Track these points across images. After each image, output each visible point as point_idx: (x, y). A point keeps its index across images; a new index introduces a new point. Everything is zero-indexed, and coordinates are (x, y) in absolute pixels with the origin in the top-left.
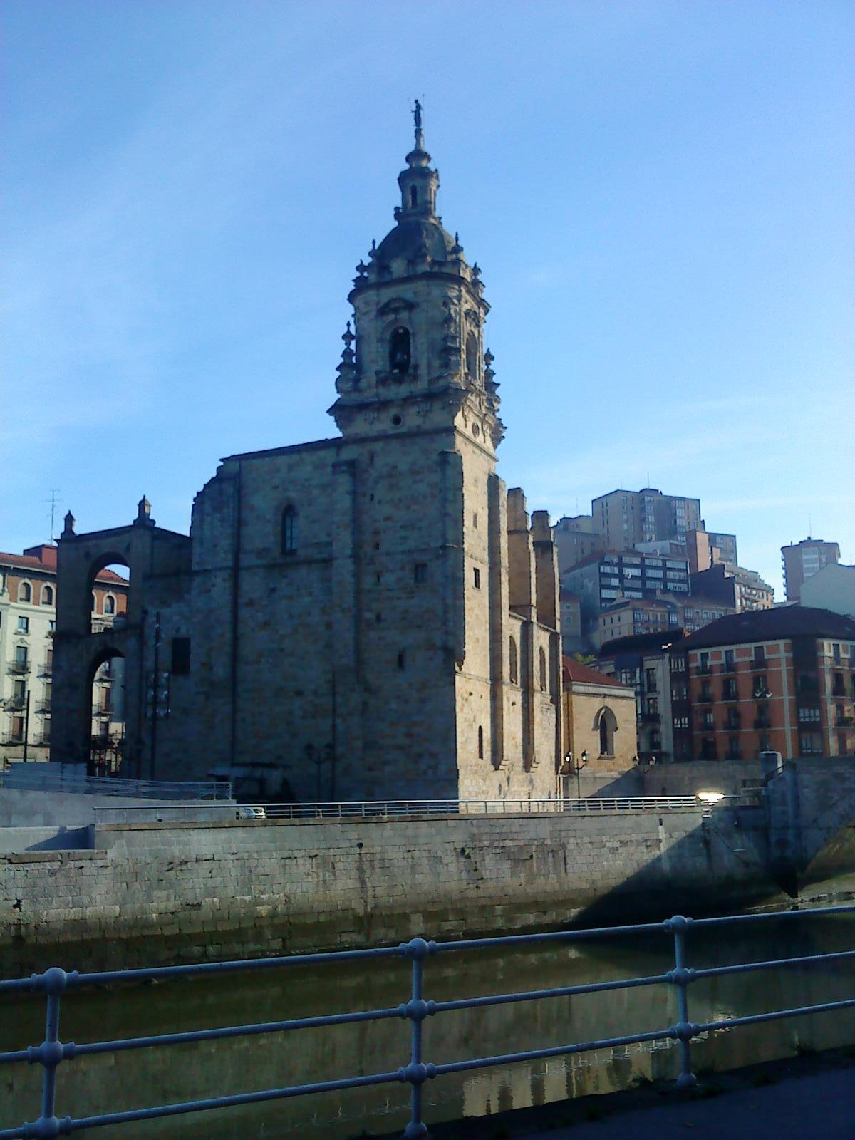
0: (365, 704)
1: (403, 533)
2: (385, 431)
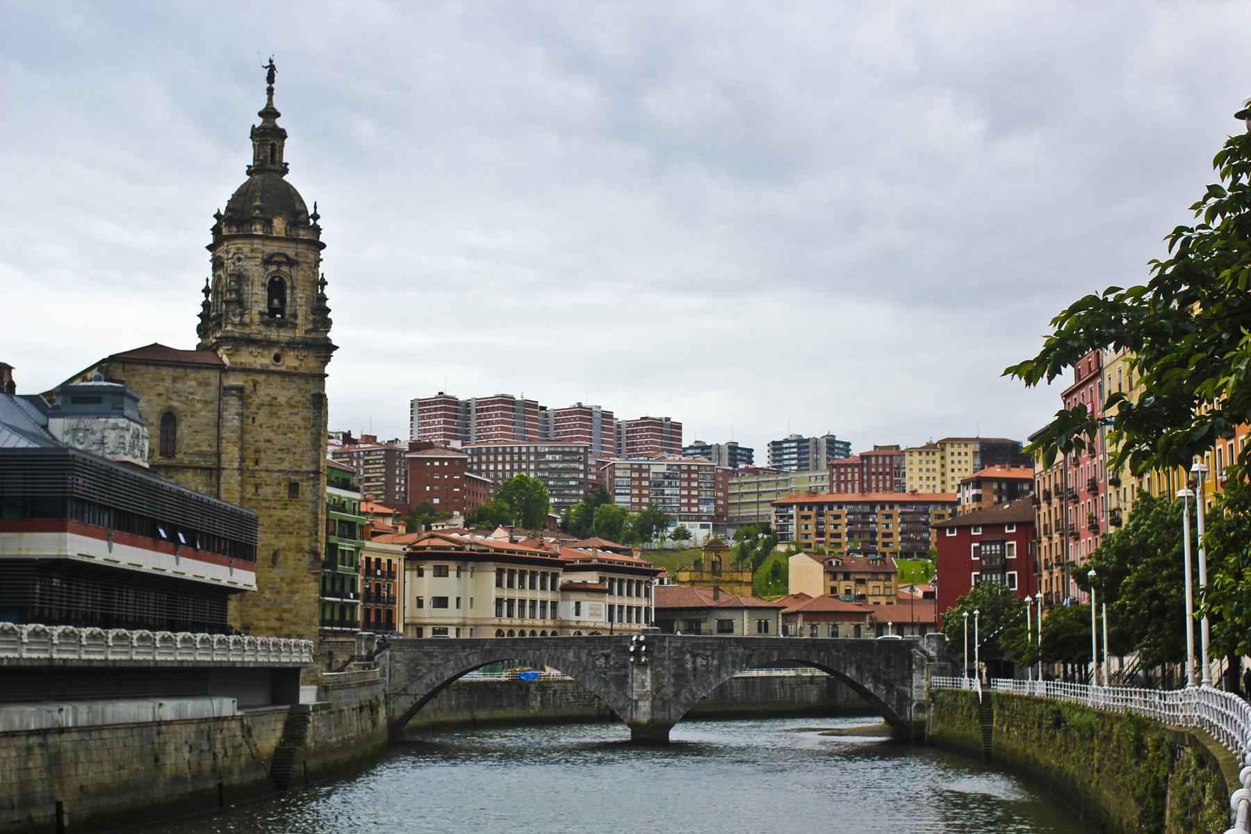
2: (266, 365)
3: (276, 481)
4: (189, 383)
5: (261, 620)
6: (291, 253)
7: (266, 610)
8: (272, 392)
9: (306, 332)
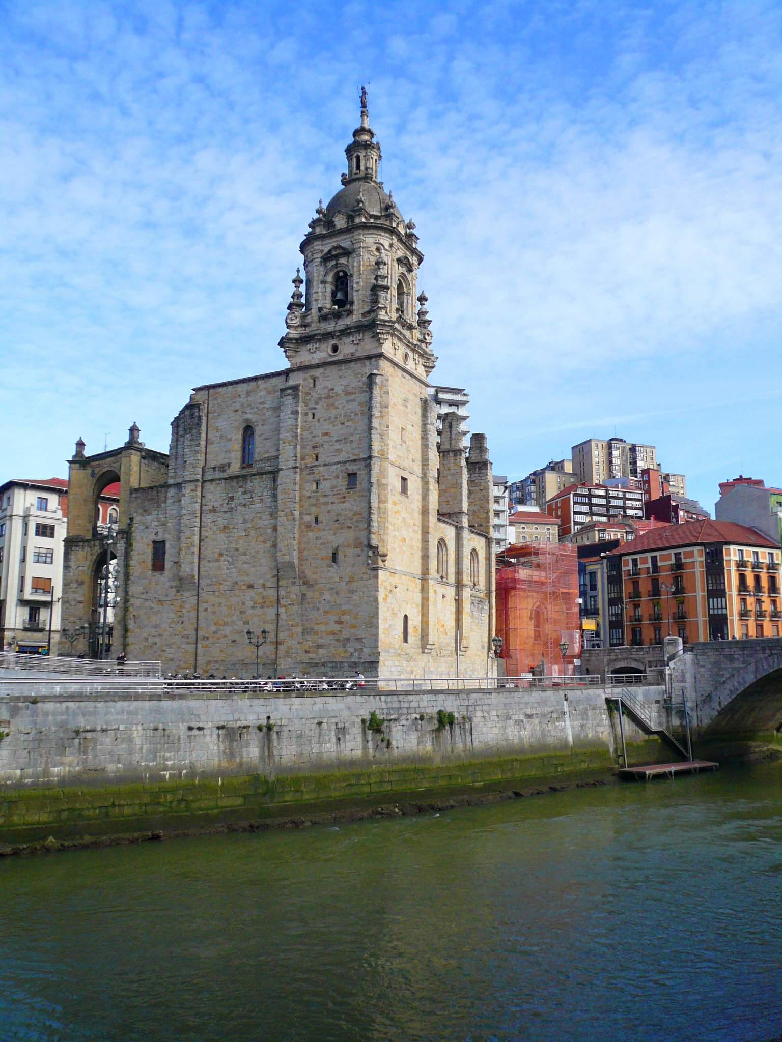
0: (304, 595)
1: (337, 446)
2: (324, 358)
3: (334, 474)
4: (259, 394)
5: (321, 623)
6: (346, 244)
7: (326, 612)
8: (329, 384)
9: (364, 315)
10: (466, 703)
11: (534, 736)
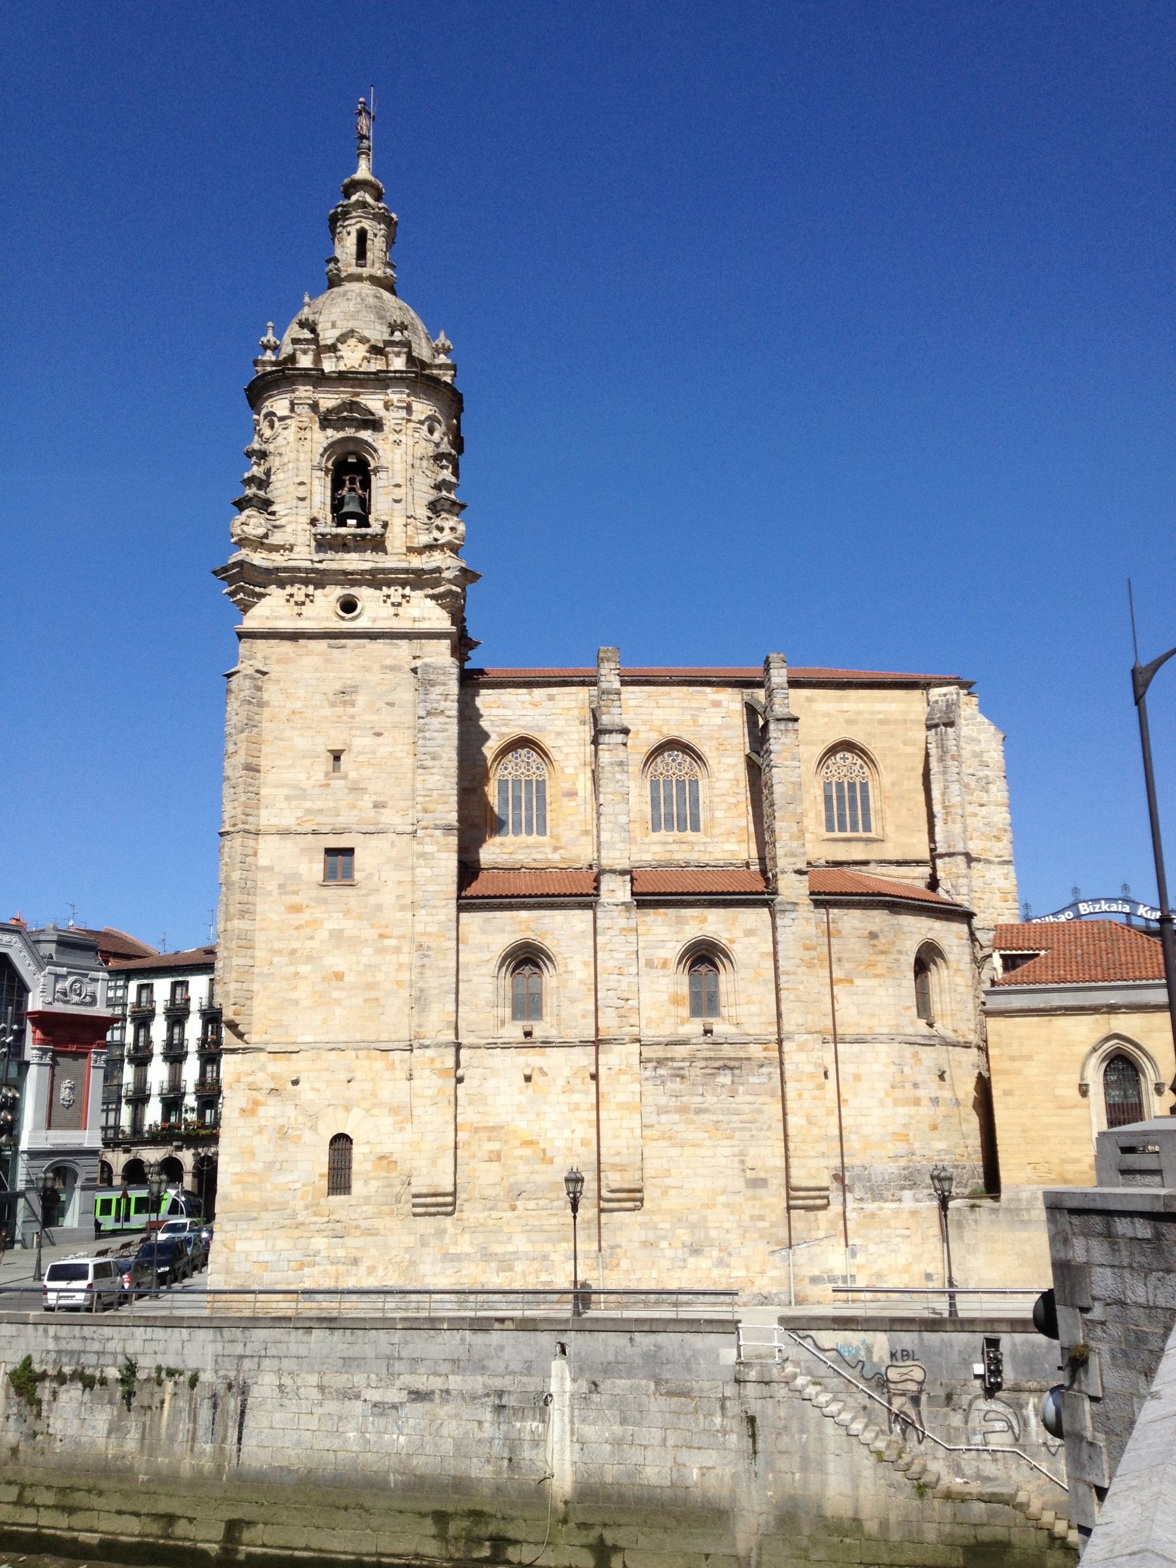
10: (239, 1349)
11: (429, 1449)
